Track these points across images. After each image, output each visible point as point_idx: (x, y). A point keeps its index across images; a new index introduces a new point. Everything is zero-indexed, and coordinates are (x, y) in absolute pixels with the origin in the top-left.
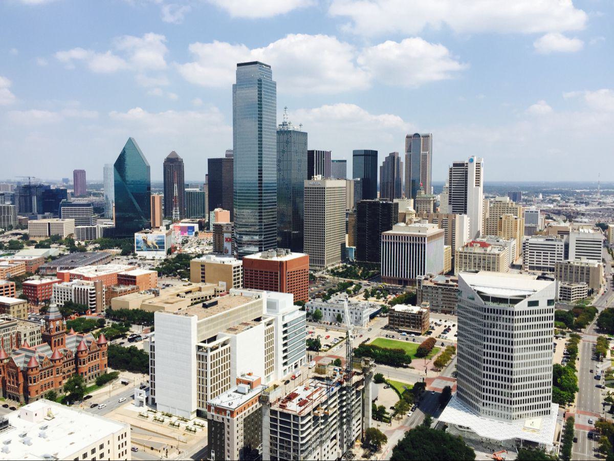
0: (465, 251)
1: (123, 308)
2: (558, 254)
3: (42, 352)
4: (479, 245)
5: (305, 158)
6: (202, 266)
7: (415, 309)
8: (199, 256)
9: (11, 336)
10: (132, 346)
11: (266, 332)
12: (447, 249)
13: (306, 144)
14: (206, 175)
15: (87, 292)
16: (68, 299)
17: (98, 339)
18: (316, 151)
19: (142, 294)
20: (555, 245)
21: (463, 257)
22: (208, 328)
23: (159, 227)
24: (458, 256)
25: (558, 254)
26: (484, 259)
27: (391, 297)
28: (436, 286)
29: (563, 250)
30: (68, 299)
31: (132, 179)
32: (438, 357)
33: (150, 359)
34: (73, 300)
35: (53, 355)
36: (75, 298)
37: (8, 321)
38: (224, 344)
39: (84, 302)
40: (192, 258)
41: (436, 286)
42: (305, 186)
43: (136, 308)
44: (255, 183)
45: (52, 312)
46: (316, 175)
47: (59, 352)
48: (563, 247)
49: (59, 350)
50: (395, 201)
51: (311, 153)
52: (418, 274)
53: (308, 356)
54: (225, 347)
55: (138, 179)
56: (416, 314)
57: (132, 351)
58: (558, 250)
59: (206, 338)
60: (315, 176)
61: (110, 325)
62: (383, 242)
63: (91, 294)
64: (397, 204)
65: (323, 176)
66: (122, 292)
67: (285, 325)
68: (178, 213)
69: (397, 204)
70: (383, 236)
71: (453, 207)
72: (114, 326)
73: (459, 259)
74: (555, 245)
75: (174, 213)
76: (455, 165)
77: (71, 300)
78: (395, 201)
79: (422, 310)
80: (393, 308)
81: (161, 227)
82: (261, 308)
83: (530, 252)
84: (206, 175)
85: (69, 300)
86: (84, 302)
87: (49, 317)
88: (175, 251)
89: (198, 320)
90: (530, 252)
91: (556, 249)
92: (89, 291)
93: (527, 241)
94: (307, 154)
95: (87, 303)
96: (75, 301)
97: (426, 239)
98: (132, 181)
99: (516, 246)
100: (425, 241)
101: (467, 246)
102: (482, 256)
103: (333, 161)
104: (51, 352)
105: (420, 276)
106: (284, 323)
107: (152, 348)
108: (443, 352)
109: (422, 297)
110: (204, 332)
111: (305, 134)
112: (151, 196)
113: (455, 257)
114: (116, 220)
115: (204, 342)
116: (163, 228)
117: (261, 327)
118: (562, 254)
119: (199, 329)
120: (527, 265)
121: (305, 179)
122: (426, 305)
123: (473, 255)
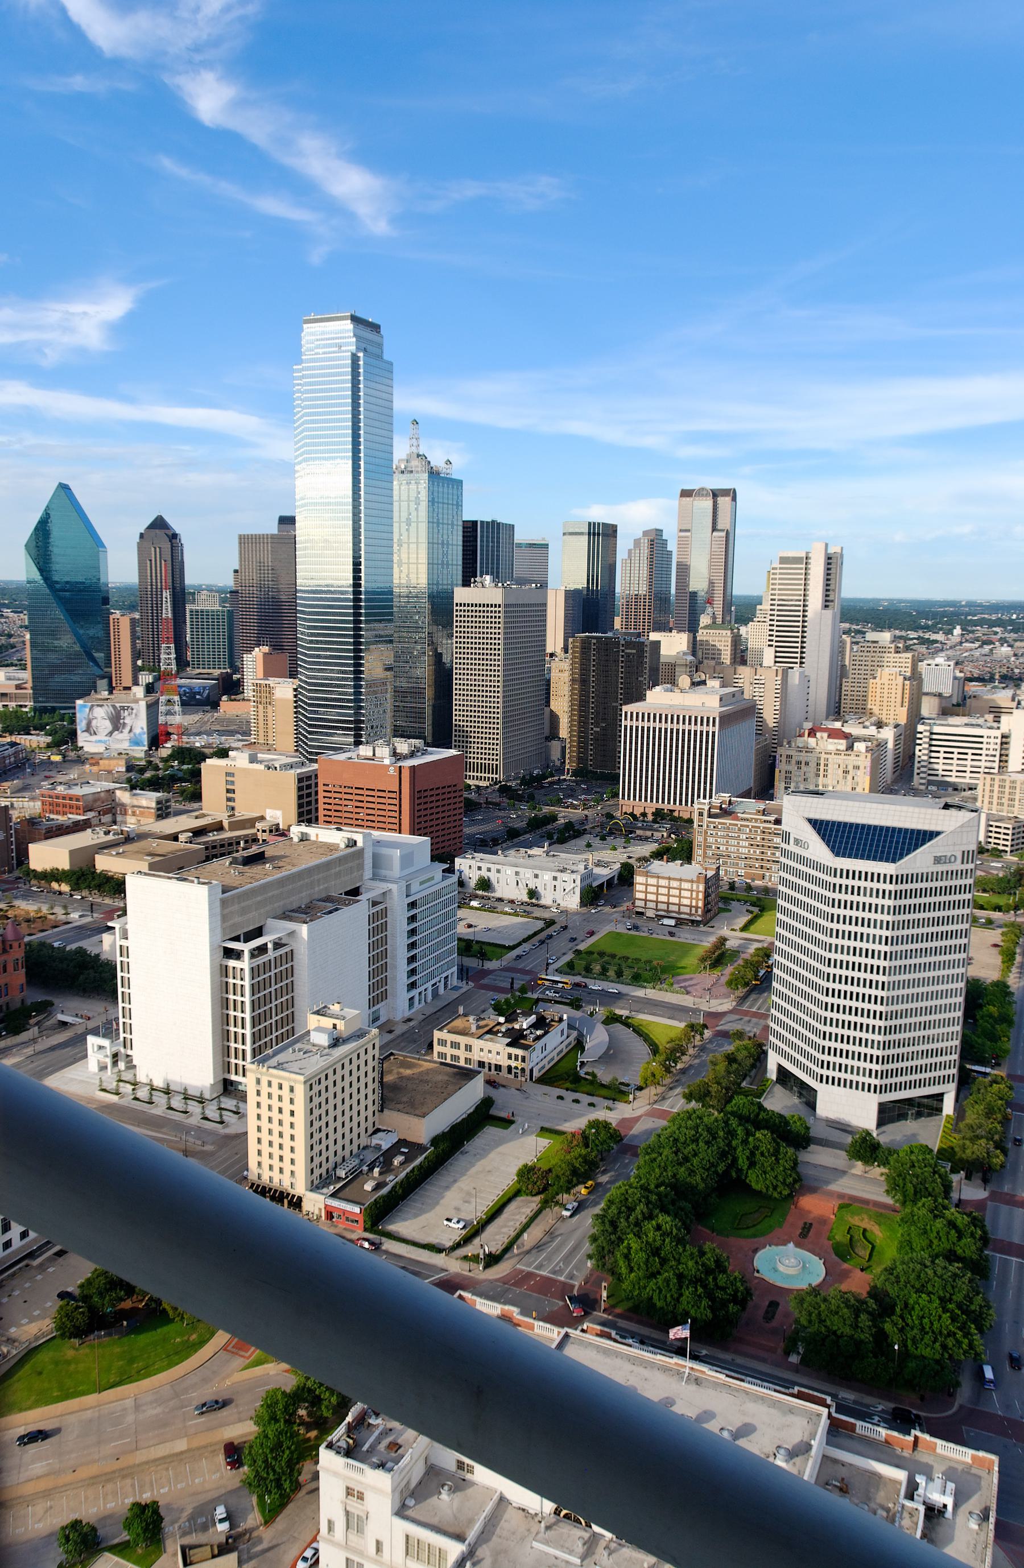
4: (825, 735)
5: (457, 538)
6: (228, 774)
8: (223, 753)
11: (373, 918)
13: (459, 505)
14: (236, 571)
18: (482, 522)
20: (982, 737)
22: (244, 911)
23: (129, 688)
31: (68, 579)
33: (119, 974)
38: (277, 945)
40: (203, 757)
42: (457, 600)
44: (346, 592)
46: (481, 576)
50: (654, 636)
51: (470, 529)
52: (699, 796)
53: (462, 970)
54: (282, 951)
55: (80, 579)
58: (988, 746)
59: (240, 932)
60: (478, 579)
62: (626, 726)
64: (657, 644)
65: (498, 577)
67: (413, 905)
68: (173, 656)
69: (657, 644)
70: (626, 713)
71: (776, 652)
74: (982, 737)
75: (163, 656)
76: (783, 560)
78: (654, 636)
81: (135, 689)
82: (361, 867)
84: (236, 571)
88: (166, 742)
89: (224, 892)
91: (984, 746)
94: (461, 528)
98: (67, 583)
99: (902, 737)
103: (519, 545)
106: (411, 899)
107: (124, 951)
110: (237, 919)
111: (460, 483)
112: (111, 617)
114: (32, 670)
115: (236, 939)
116: (139, 691)
117: (359, 912)
119: (226, 911)
121: (457, 585)
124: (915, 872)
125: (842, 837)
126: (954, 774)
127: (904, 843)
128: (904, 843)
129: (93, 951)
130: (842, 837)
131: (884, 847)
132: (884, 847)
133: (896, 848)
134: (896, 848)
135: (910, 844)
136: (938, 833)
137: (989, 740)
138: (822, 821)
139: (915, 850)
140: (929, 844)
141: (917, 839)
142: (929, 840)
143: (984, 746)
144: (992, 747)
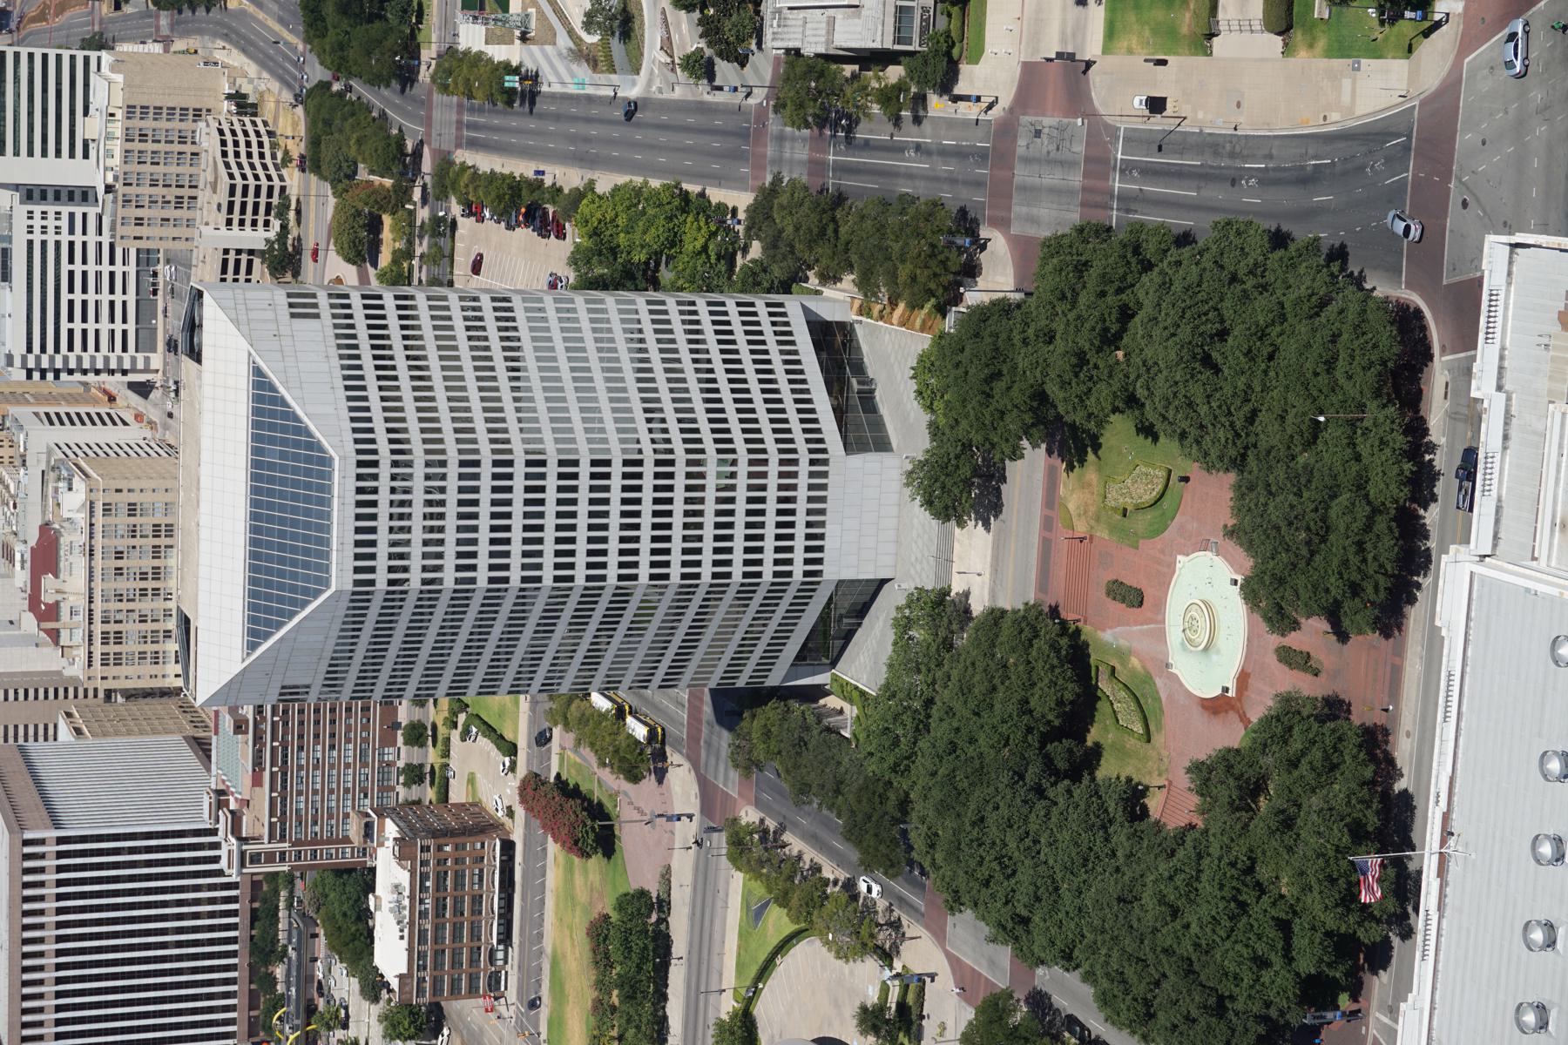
0: (79, 636)
2: (72, 232)
4: (48, 581)
7: (391, 874)
12: (78, 731)
20: (30, 243)
21: (112, 648)
24: (112, 671)
25: (72, 232)
26: (119, 555)
27: (344, 985)
28: (267, 775)
29: (51, 209)
32: (603, 764)
41: (267, 775)
48: (37, 209)
56: (412, 873)
58: (51, 230)
73: (123, 670)
74: (30, 243)
79: (390, 843)
80: (395, 984)
83: (71, 348)
90: (71, 348)
91: (51, 238)
93: (17, 362)
97: (28, 835)
99: (42, 410)
100: (42, 842)
101: (54, 635)
102: (98, 562)
105: (223, 853)
108: (578, 742)
109: (330, 841)
113: (111, 684)
118: (72, 216)
120: (134, 360)
122: (368, 827)
123: (98, 606)
124: (346, 415)
125: (281, 574)
126: (118, 298)
127: (284, 442)
128: (284, 442)
130: (281, 574)
131: (295, 484)
132: (295, 484)
133: (296, 457)
134: (296, 457)
135: (284, 429)
136: (258, 372)
137: (37, 230)
138: (253, 620)
139: (297, 419)
140: (282, 390)
141: (273, 414)
142: (272, 388)
143: (51, 238)
144: (51, 223)
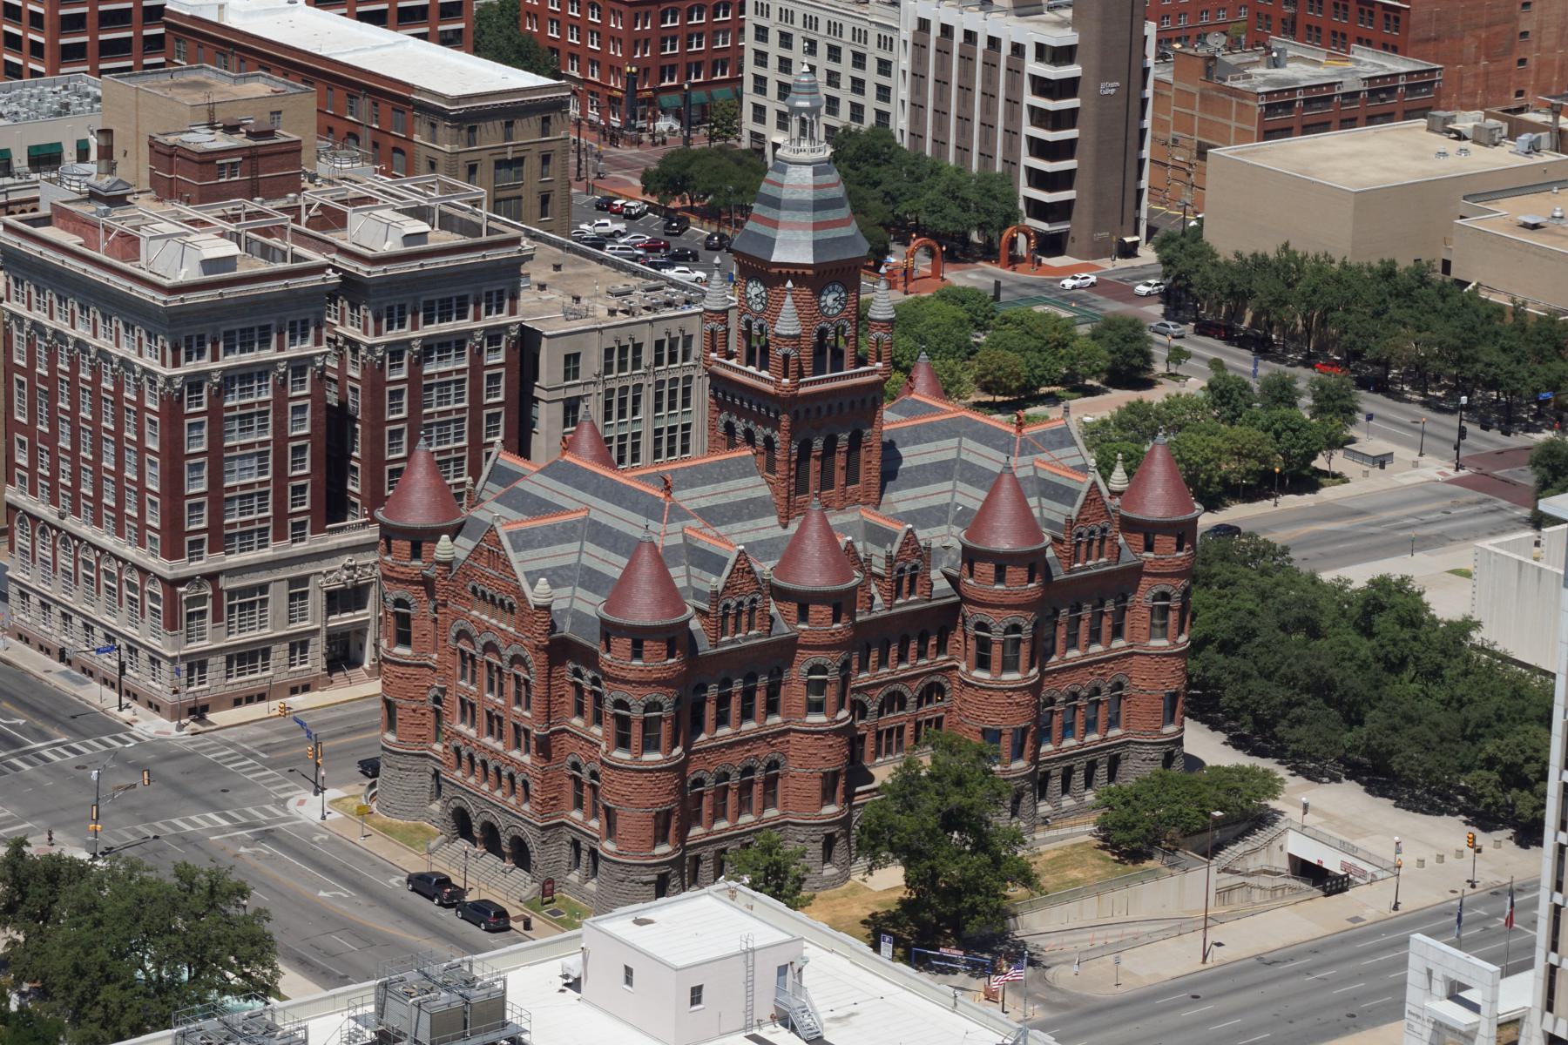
1: (1298, 247)
3: (712, 516)
9: (477, 366)
10: (1381, 584)
15: (1015, 71)
16: (857, 112)
17: (1119, 478)
19: (1460, 136)
30: (857, 112)
34: (900, 122)
35: (791, 554)
36: (917, 107)
37: (456, 239)
39: (987, 157)
43: (1404, 263)
45: (798, 206)
47: (829, 533)
49: (835, 519)
57: (1381, 622)
61: (1195, 386)
63: (1043, 87)
66: (1289, 106)
72: (1225, 394)
77: (882, 116)
85: (870, 119)
86: (987, 157)
87: (770, 243)
92: (1032, 66)
95: (1011, 162)
96: (917, 136)
104: (768, 528)
129: (1445, 605)
